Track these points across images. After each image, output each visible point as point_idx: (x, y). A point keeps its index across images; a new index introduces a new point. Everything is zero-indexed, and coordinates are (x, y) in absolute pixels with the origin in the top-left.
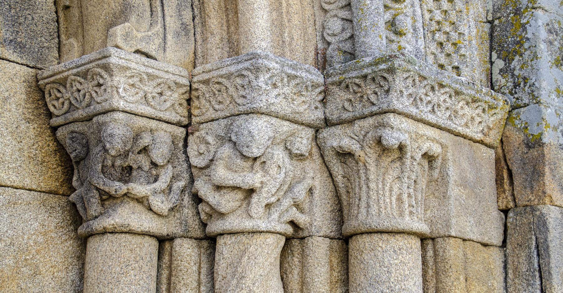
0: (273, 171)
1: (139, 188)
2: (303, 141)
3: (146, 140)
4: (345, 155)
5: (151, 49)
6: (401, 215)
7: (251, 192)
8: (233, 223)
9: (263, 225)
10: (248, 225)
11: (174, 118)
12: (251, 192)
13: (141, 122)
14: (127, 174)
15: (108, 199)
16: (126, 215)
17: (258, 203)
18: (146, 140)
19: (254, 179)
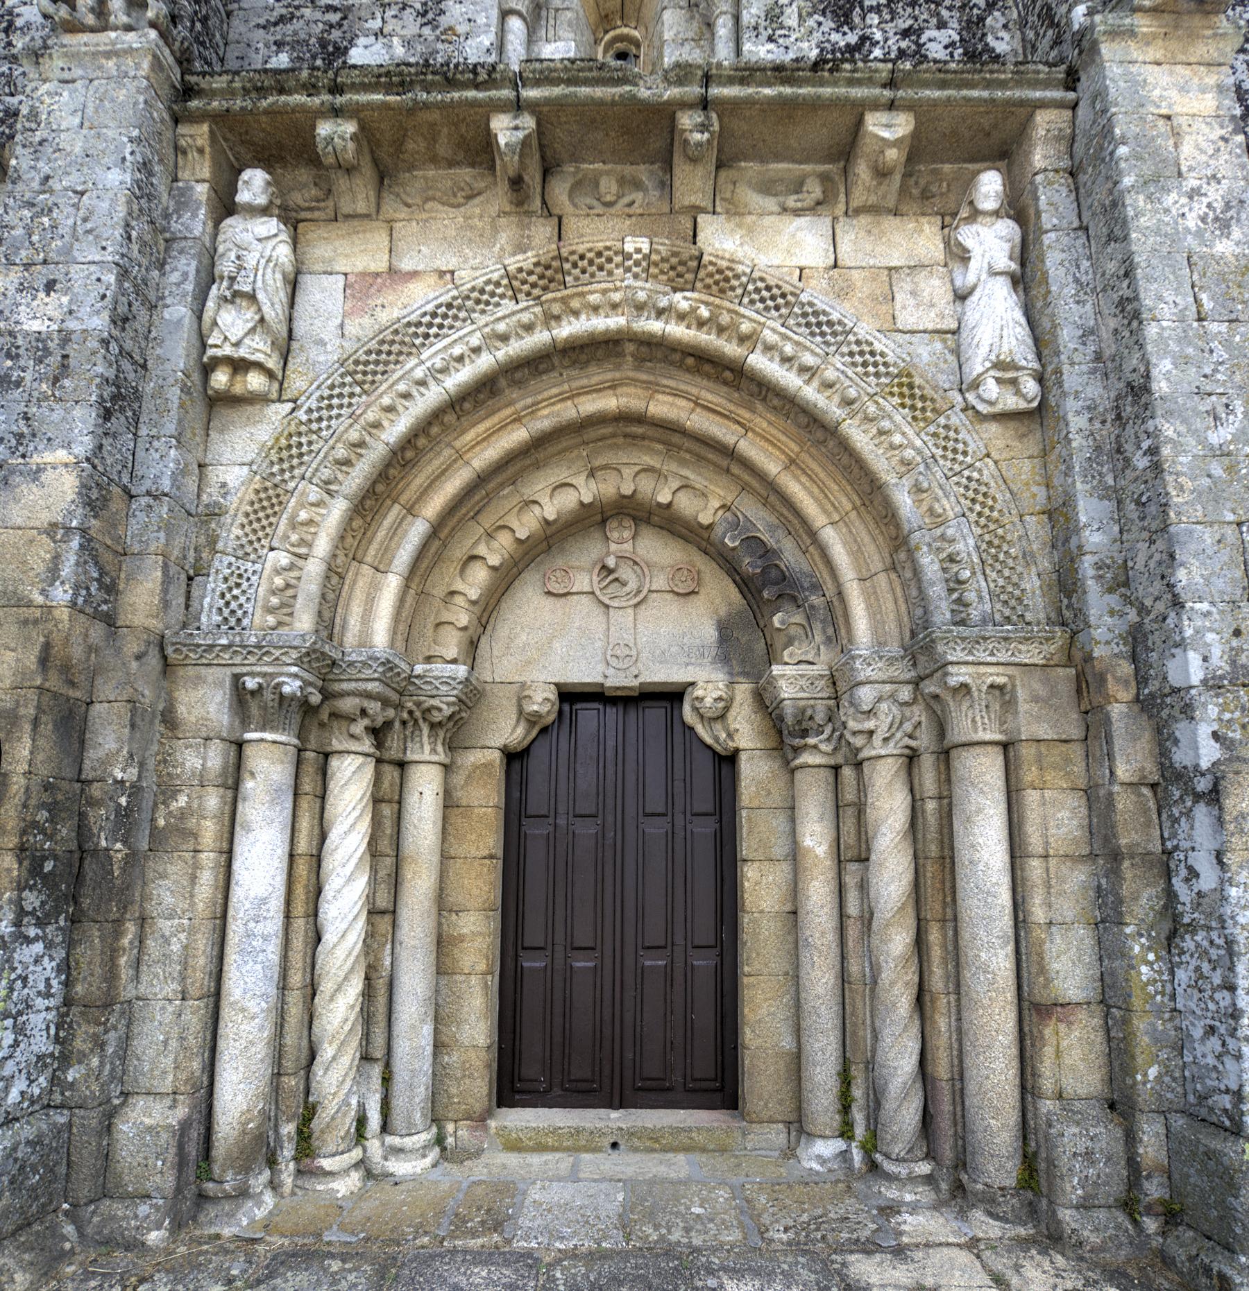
0: (882, 717)
1: (811, 741)
2: (905, 693)
3: (809, 712)
4: (936, 697)
5: (810, 657)
6: (976, 731)
7: (871, 733)
8: (865, 753)
9: (883, 752)
10: (873, 753)
11: (824, 695)
12: (871, 733)
13: (803, 703)
14: (805, 733)
15: (797, 750)
16: (807, 758)
17: (877, 740)
18: (809, 712)
19: (870, 725)
